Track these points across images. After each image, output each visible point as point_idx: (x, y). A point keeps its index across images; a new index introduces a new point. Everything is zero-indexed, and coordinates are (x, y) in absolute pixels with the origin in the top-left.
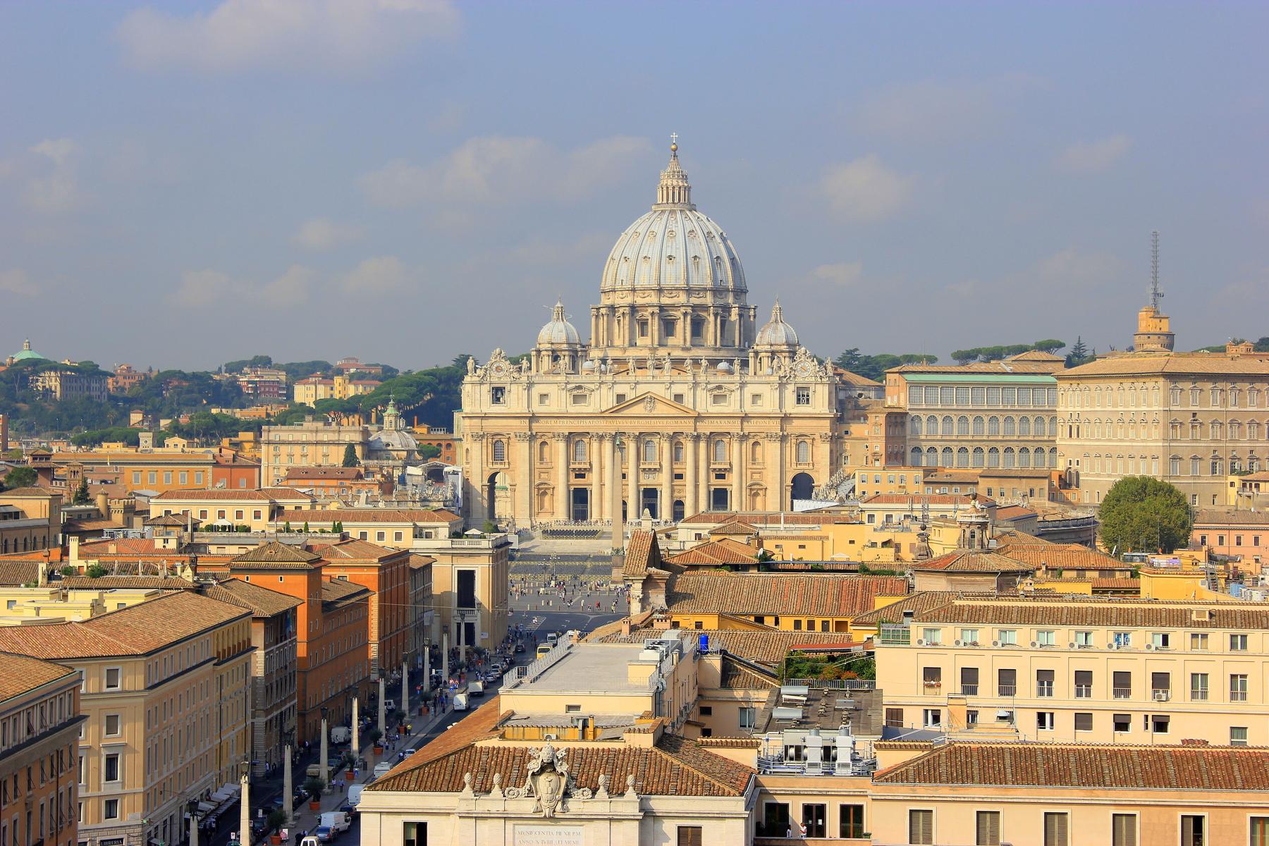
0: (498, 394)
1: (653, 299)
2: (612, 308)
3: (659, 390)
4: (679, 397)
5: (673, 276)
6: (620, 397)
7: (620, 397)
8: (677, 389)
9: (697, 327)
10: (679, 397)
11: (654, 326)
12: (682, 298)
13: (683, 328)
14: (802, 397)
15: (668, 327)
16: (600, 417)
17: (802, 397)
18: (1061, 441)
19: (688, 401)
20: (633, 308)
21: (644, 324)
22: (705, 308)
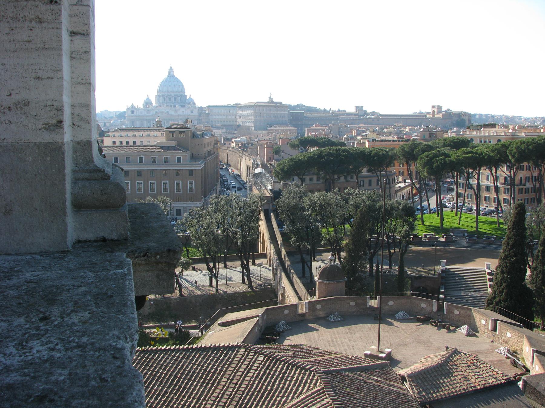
0: (133, 112)
1: (167, 94)
2: (159, 96)
3: (163, 110)
4: (168, 112)
5: (170, 89)
6: (156, 112)
7: (156, 112)
8: (168, 110)
9: (175, 99)
10: (168, 112)
11: (167, 99)
12: (173, 94)
13: (173, 99)
14: (192, 112)
15: (170, 99)
16: (152, 116)
17: (192, 112)
18: (238, 119)
19: (170, 113)
20: (163, 95)
21: (165, 99)
22: (177, 95)
